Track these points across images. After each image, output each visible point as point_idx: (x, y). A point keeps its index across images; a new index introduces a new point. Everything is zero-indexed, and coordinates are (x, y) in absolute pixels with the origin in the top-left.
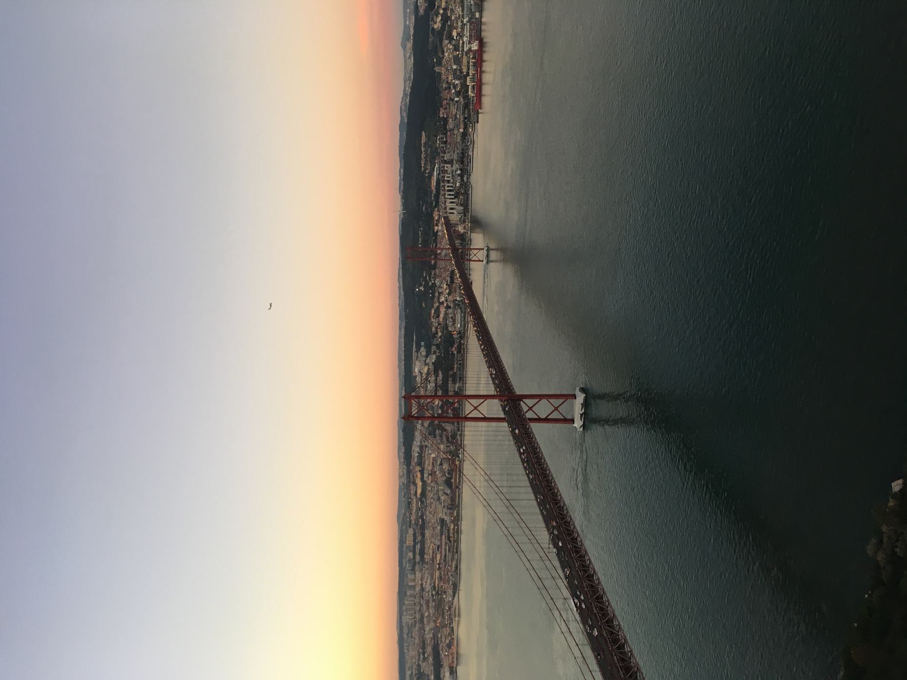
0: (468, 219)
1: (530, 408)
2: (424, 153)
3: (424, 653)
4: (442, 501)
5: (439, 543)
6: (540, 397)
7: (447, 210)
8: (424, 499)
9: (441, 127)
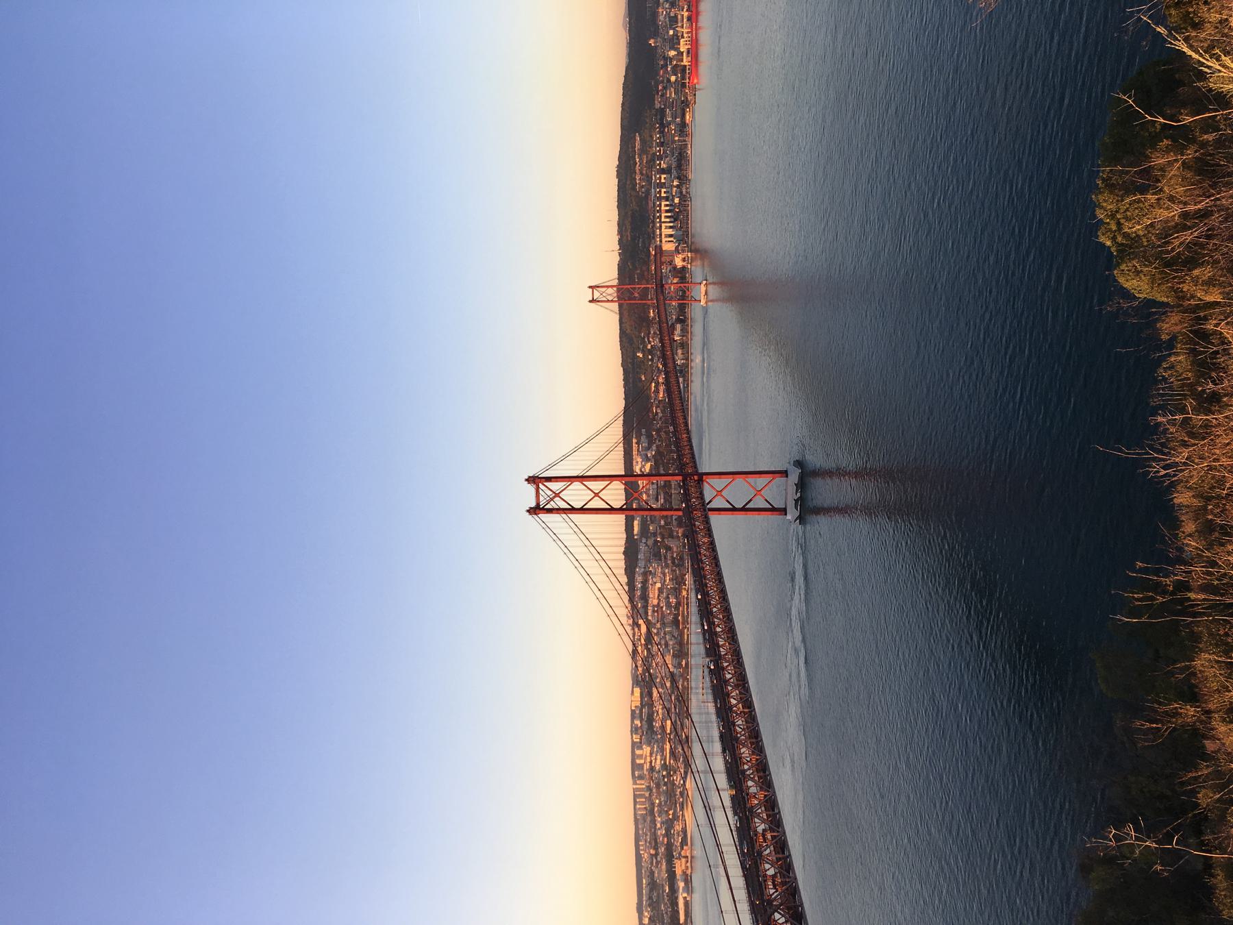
0: (688, 246)
3: (656, 855)
4: (671, 647)
7: (663, 236)
8: (649, 646)
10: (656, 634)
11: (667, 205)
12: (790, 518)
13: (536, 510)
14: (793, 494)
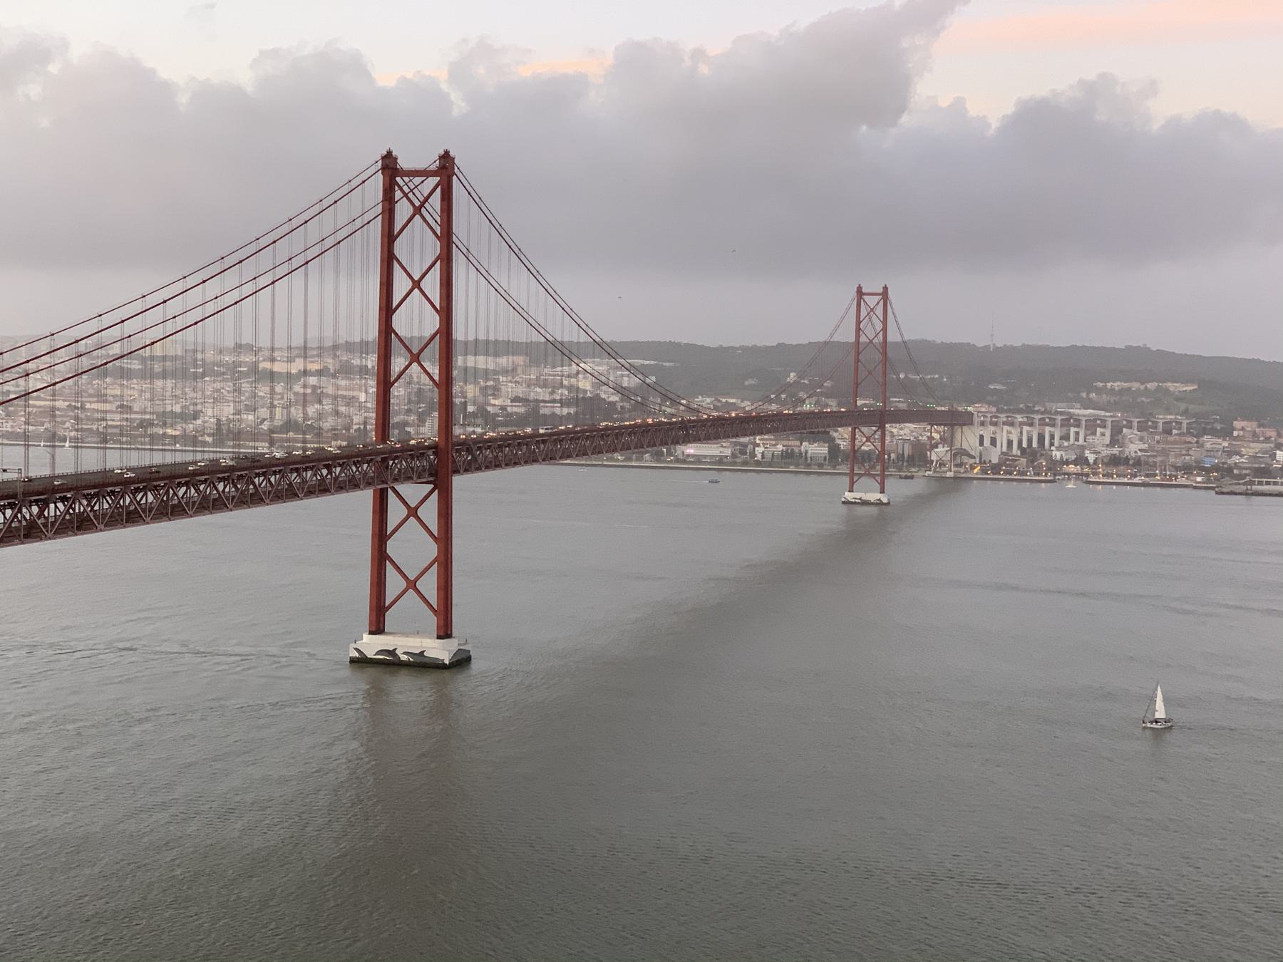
0: (965, 472)
1: (413, 512)
2: (1142, 387)
5: (136, 408)
6: (444, 538)
7: (992, 428)
9: (1207, 424)
10: (273, 392)
11: (1052, 437)
12: (364, 640)
13: (389, 166)
14: (404, 644)
